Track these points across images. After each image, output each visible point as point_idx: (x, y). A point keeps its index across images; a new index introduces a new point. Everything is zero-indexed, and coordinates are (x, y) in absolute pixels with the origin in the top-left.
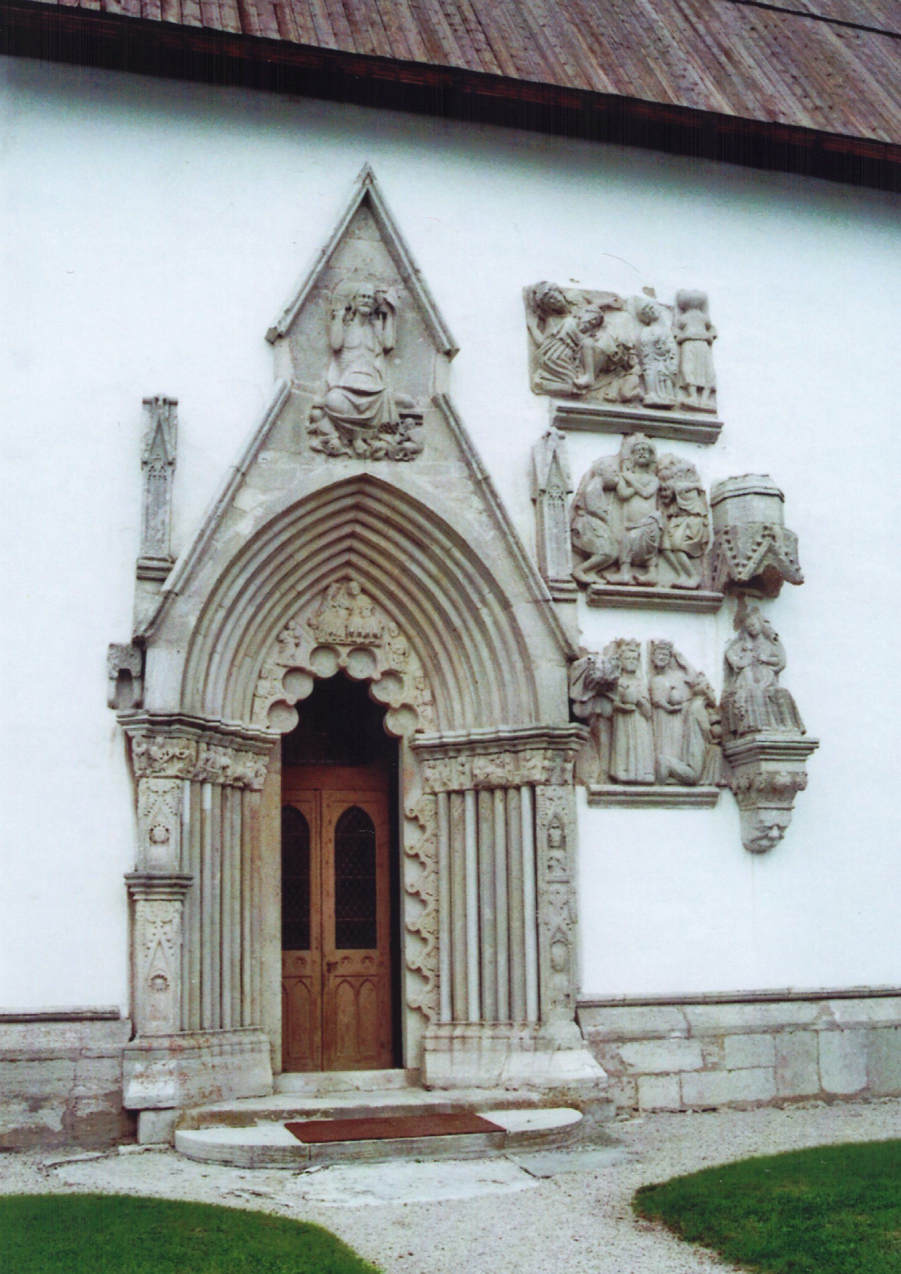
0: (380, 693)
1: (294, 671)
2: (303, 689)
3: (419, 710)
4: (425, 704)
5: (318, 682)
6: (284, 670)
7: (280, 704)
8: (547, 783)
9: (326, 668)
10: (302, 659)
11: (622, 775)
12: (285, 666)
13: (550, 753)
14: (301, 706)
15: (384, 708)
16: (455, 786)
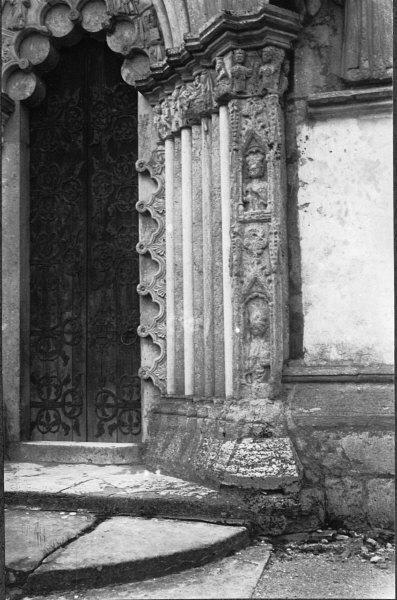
0: (114, 44)
1: (27, 35)
2: (40, 51)
3: (148, 52)
4: (154, 44)
5: (55, 41)
6: (16, 34)
7: (15, 71)
8: (241, 95)
9: (61, 26)
10: (33, 18)
11: (351, 76)
12: (15, 29)
13: (239, 53)
14: (35, 69)
15: (118, 60)
16: (174, 128)
